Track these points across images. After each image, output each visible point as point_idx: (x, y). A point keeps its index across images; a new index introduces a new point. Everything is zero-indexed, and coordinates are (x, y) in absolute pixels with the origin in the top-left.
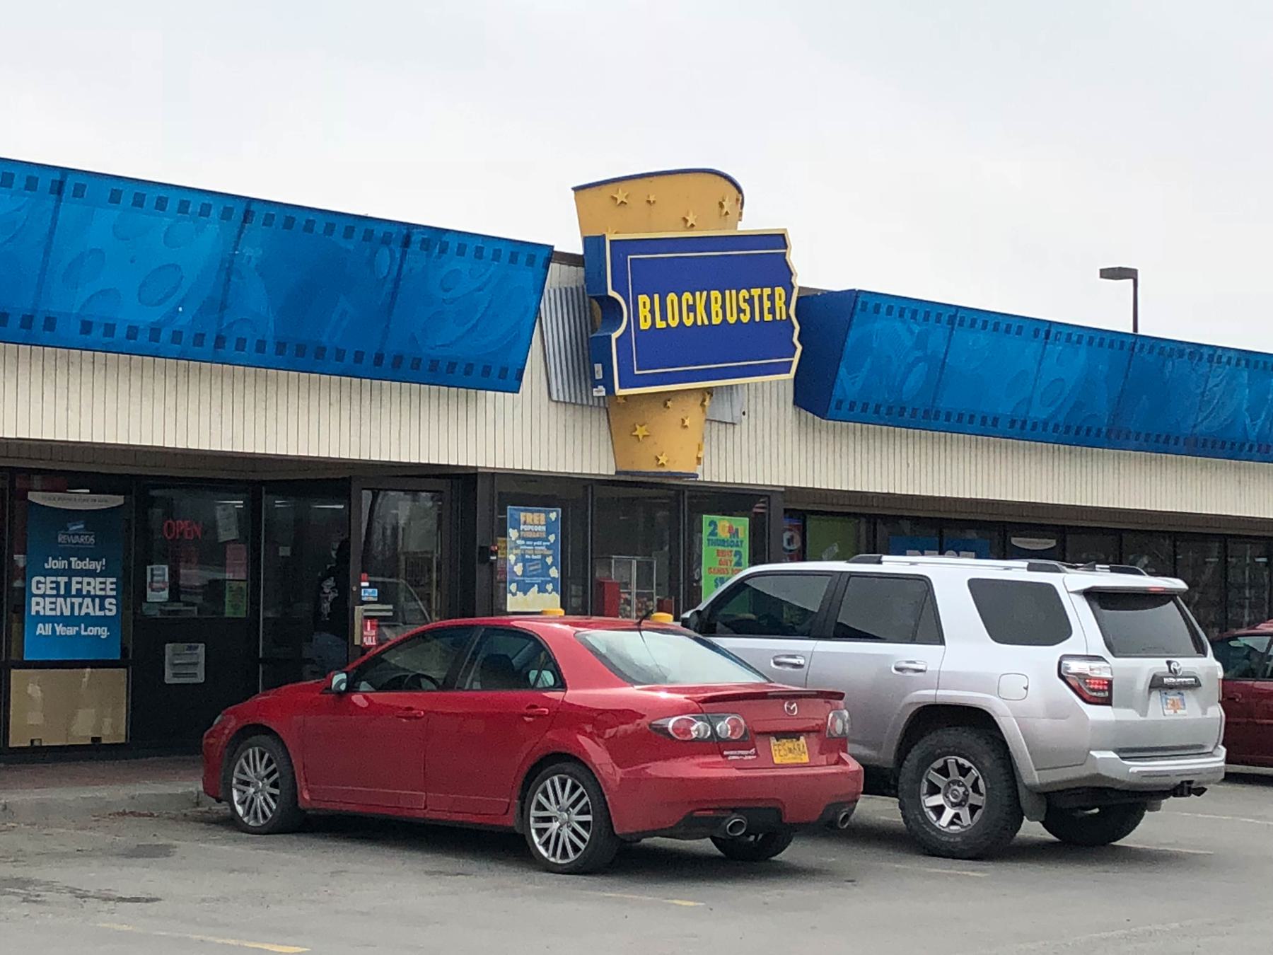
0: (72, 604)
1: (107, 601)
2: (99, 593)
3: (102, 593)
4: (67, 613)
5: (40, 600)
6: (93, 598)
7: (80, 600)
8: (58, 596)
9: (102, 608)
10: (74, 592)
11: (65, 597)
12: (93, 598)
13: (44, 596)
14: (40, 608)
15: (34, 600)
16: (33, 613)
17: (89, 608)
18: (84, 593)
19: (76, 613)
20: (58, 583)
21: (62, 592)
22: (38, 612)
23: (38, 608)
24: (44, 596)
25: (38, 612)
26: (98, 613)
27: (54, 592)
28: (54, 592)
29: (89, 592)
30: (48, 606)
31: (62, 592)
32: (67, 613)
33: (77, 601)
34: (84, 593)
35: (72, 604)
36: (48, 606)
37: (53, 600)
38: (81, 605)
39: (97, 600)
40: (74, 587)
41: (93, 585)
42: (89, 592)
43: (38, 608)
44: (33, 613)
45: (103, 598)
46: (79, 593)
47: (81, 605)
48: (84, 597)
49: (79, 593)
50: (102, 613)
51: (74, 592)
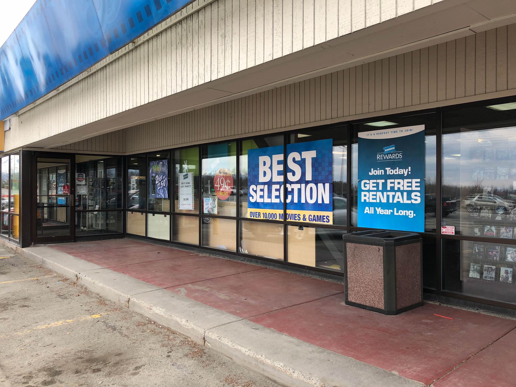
0: (388, 196)
1: (413, 194)
2: (406, 189)
3: (410, 189)
4: (384, 201)
5: (367, 193)
6: (402, 192)
7: (394, 193)
8: (378, 190)
9: (409, 198)
10: (389, 189)
11: (382, 192)
12: (402, 192)
13: (369, 191)
14: (366, 198)
15: (363, 193)
16: (363, 201)
17: (399, 198)
18: (396, 189)
19: (391, 201)
20: (378, 184)
21: (380, 188)
22: (365, 200)
23: (365, 198)
24: (369, 191)
25: (365, 200)
26: (406, 201)
27: (375, 189)
28: (375, 189)
29: (399, 188)
30: (371, 197)
31: (380, 188)
32: (384, 201)
33: (391, 194)
34: (396, 189)
35: (388, 196)
36: (371, 197)
37: (375, 193)
38: (394, 196)
39: (405, 194)
40: (389, 186)
41: (404, 184)
42: (399, 188)
43: (365, 198)
44: (363, 201)
45: (409, 193)
46: (392, 189)
47: (394, 196)
48: (396, 191)
49: (392, 189)
50: (409, 202)
51: (389, 189)
